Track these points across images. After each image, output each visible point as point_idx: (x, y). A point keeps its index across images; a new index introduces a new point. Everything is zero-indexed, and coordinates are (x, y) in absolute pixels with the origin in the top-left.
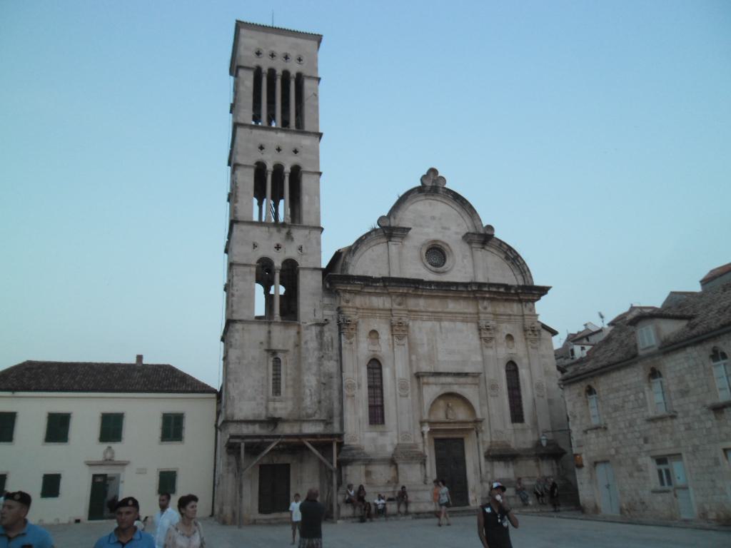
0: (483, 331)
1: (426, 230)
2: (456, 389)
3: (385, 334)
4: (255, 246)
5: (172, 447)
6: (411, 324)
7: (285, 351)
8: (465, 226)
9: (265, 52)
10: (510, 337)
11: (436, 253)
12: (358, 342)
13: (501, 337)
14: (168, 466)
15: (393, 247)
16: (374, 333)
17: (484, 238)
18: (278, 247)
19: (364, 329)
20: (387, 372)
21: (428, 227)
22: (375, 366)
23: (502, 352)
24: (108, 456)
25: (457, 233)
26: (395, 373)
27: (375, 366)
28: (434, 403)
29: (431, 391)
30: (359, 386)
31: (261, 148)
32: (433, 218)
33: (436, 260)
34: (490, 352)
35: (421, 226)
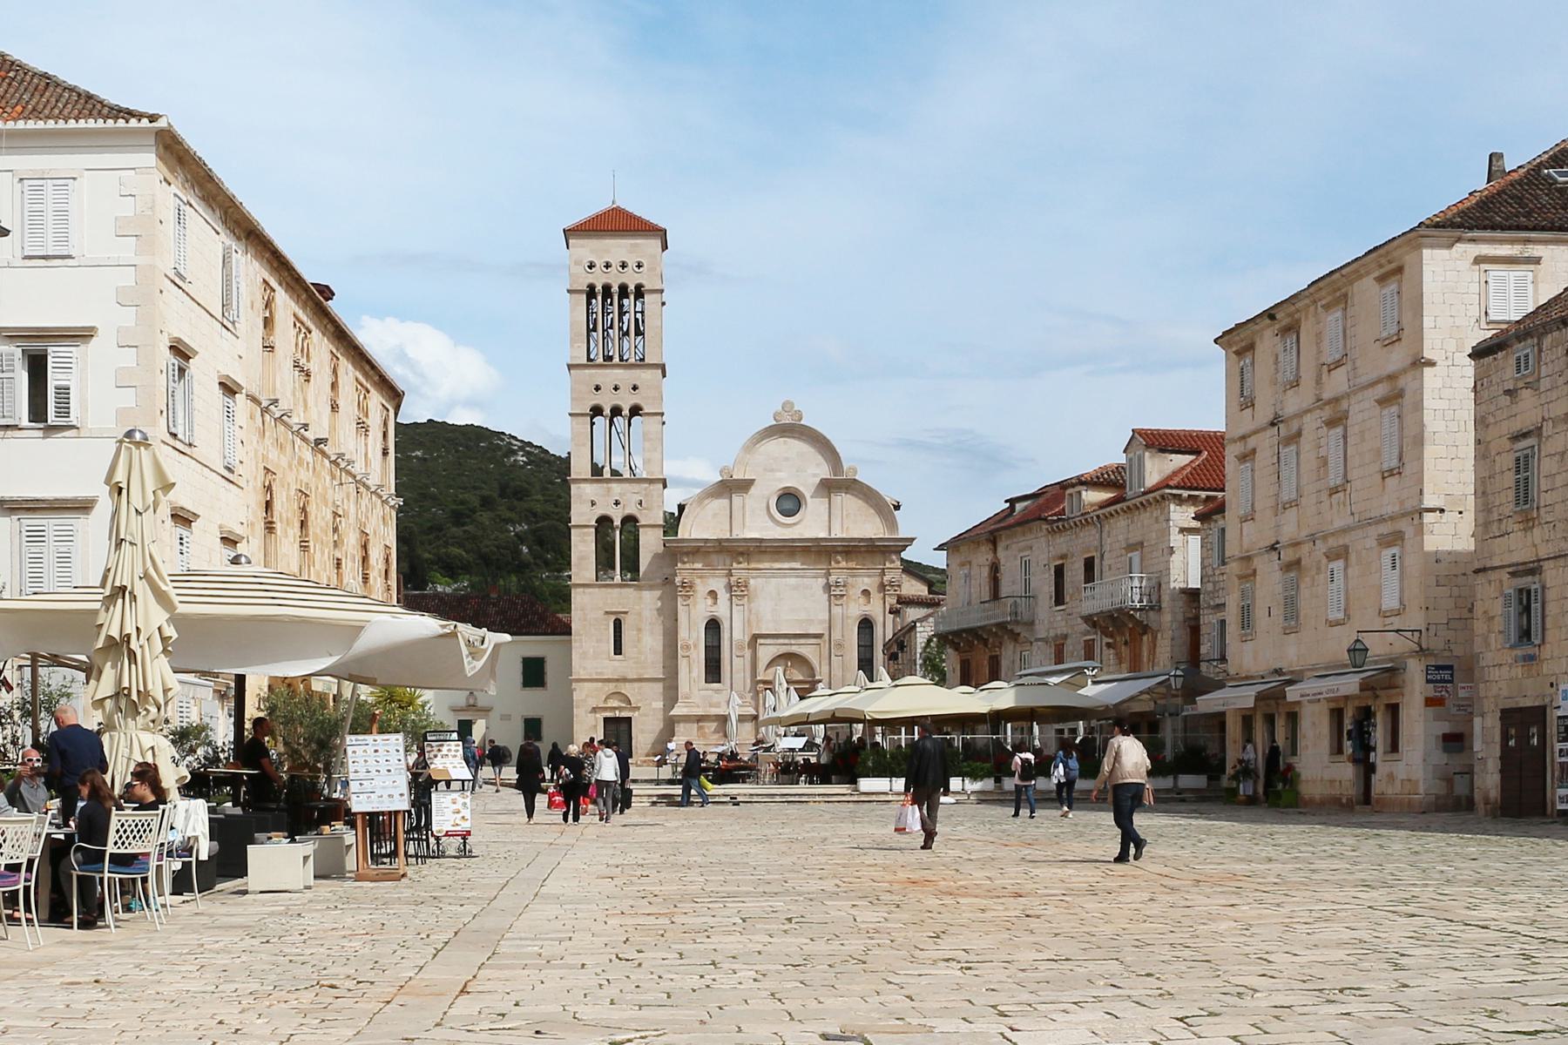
0: (833, 588)
1: (778, 475)
2: (794, 649)
3: (723, 596)
4: (593, 504)
5: (534, 693)
6: (752, 582)
7: (626, 613)
8: (824, 471)
9: (600, 263)
10: (866, 593)
11: (790, 502)
12: (695, 603)
13: (855, 592)
14: (531, 714)
15: (736, 499)
16: (713, 594)
17: (837, 485)
18: (617, 503)
19: (702, 588)
20: (725, 635)
21: (780, 471)
22: (713, 626)
23: (855, 609)
24: (471, 702)
25: (815, 475)
26: (735, 633)
27: (713, 626)
28: (770, 665)
29: (766, 652)
30: (695, 646)
31: (597, 388)
32: (787, 459)
33: (788, 505)
34: (837, 610)
35: (772, 470)
